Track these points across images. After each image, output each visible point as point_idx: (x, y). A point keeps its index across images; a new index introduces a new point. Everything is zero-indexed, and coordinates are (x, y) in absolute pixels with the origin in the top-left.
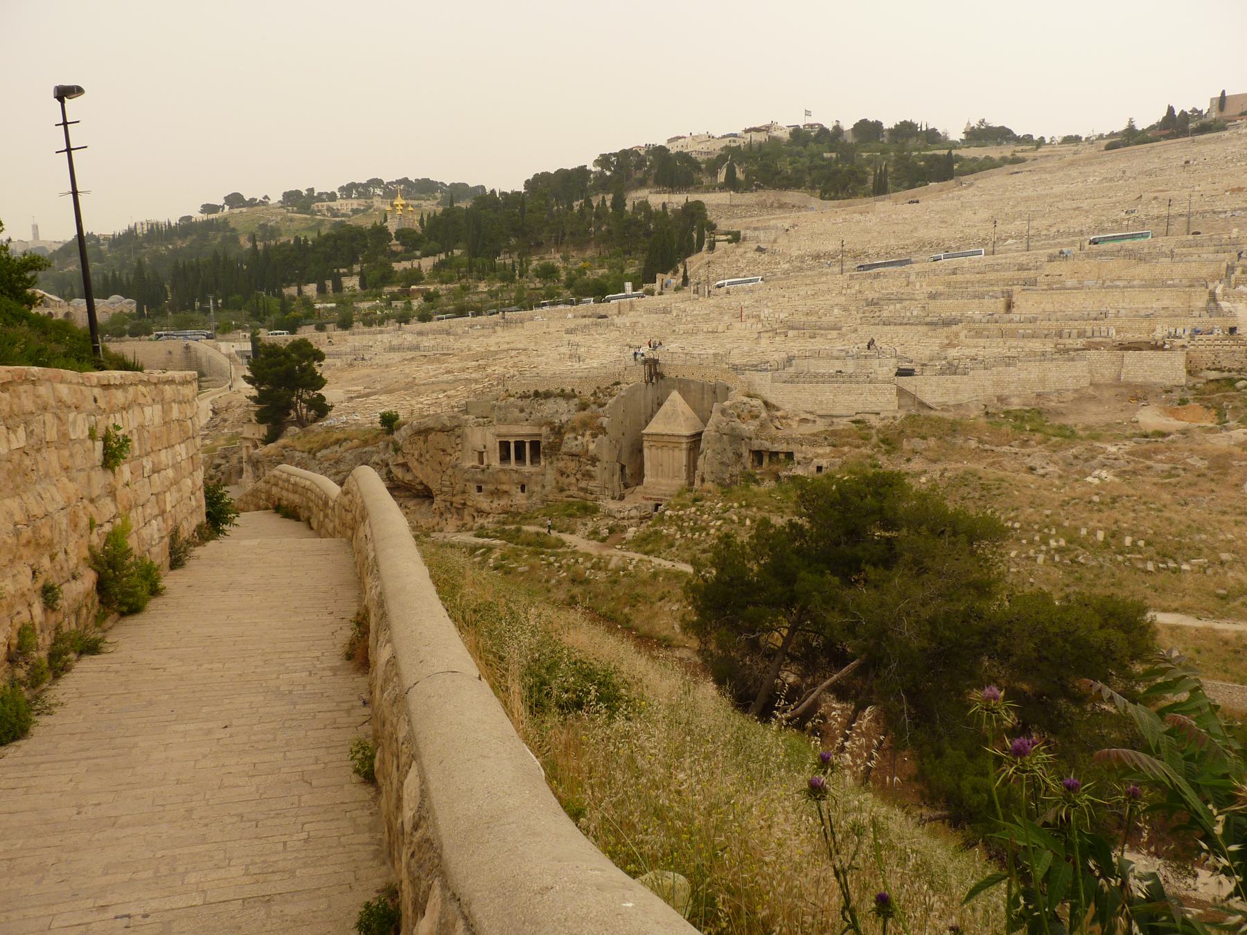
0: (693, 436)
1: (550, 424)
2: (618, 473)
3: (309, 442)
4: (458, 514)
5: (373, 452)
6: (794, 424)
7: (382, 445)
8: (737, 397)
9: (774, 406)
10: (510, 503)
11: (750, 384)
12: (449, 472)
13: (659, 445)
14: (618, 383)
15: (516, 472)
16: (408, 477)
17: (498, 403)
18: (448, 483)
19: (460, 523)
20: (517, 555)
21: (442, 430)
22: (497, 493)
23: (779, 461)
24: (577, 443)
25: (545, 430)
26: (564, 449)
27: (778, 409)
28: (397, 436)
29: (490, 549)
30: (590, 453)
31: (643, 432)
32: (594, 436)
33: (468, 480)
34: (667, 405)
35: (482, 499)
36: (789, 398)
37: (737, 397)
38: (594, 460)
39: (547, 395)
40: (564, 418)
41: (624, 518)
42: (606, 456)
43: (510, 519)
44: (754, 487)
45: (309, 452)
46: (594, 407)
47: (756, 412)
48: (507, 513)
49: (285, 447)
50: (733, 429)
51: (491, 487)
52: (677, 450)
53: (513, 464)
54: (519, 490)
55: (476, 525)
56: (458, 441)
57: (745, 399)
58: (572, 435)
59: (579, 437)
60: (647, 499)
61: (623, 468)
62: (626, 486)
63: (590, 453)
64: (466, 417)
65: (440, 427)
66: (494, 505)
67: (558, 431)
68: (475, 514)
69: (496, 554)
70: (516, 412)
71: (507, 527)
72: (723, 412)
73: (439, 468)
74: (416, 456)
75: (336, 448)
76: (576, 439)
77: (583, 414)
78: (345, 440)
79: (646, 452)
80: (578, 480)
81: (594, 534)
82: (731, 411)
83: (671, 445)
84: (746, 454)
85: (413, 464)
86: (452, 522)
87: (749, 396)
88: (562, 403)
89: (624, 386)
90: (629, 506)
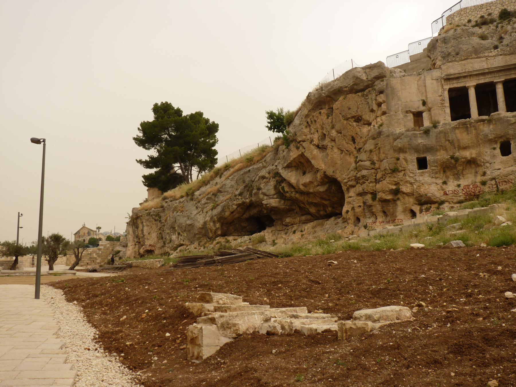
10: (479, 179)
18: (368, 163)
33: (401, 150)
51: (443, 156)
54: (498, 151)
56: (381, 98)
66: (451, 186)
70: (476, 40)
73: (351, 147)
75: (217, 180)
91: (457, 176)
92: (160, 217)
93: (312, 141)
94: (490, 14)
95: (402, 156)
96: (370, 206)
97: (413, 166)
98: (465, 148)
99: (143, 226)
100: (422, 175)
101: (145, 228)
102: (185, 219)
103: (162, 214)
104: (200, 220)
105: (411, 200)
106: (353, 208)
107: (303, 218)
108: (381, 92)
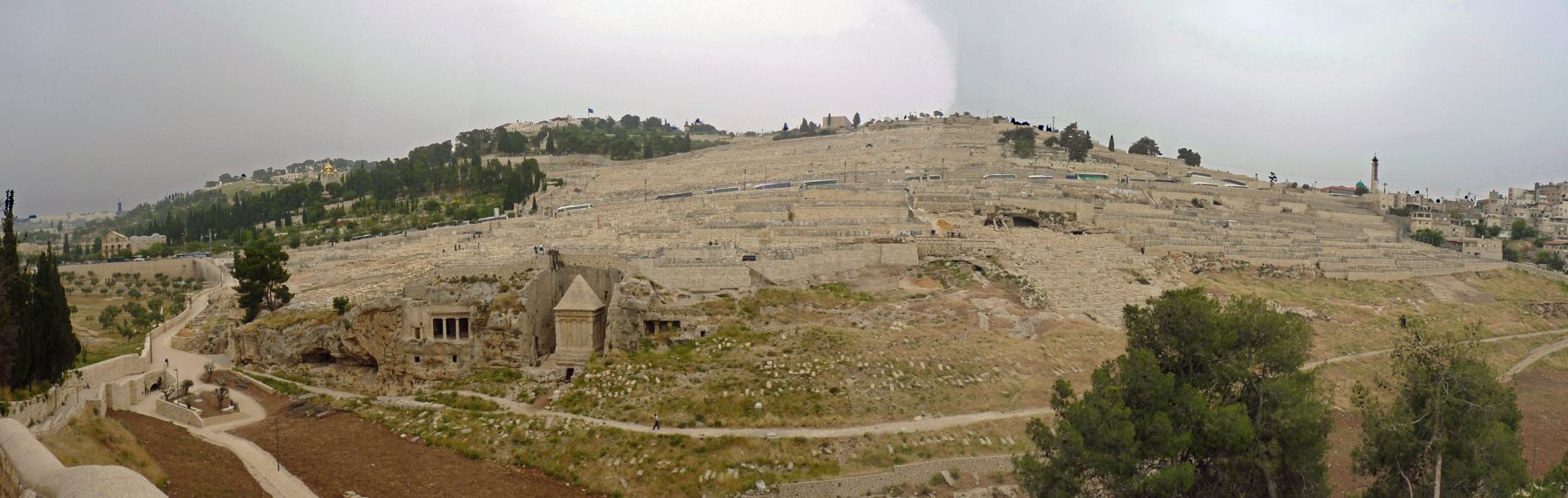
0: (597, 311)
1: (477, 304)
2: (533, 344)
3: (277, 322)
4: (399, 380)
5: (327, 329)
6: (675, 299)
7: (334, 323)
8: (629, 279)
9: (658, 286)
10: (443, 371)
11: (637, 269)
12: (392, 345)
13: (569, 319)
14: (531, 270)
15: (449, 345)
16: (357, 349)
17: (432, 287)
18: (391, 355)
19: (400, 388)
20: (457, 417)
22: (432, 363)
23: (668, 329)
24: (501, 319)
25: (473, 309)
26: (490, 324)
27: (661, 288)
28: (346, 316)
29: (432, 412)
30: (513, 327)
31: (555, 308)
32: (516, 313)
33: (407, 352)
34: (573, 287)
35: (419, 368)
36: (668, 279)
37: (629, 279)
38: (517, 333)
39: (473, 280)
40: (489, 299)
41: (544, 382)
42: (525, 330)
43: (445, 385)
44: (651, 350)
45: (277, 329)
46: (513, 289)
47: (646, 291)
48: (441, 380)
49: (259, 325)
50: (631, 304)
51: (427, 358)
52: (584, 323)
53: (445, 338)
55: (414, 391)
56: (399, 319)
57: (636, 280)
58: (497, 313)
59: (503, 314)
60: (560, 365)
61: (537, 338)
62: (539, 355)
63: (513, 327)
64: (406, 299)
66: (430, 373)
67: (484, 310)
68: (414, 381)
69: (438, 417)
70: (448, 294)
71: (443, 392)
72: (622, 290)
73: (382, 341)
75: (298, 326)
76: (500, 316)
77: (504, 295)
78: (305, 319)
79: (557, 325)
80: (502, 351)
81: (522, 397)
82: (627, 290)
83: (578, 319)
84: (641, 324)
85: (361, 338)
86: (394, 387)
87: (638, 278)
88: (486, 287)
89: (536, 272)
90: (548, 371)
91: (434, 367)
93: (361, 331)
95: (407, 355)
98: (438, 355)
104: (289, 352)
108: (399, 315)
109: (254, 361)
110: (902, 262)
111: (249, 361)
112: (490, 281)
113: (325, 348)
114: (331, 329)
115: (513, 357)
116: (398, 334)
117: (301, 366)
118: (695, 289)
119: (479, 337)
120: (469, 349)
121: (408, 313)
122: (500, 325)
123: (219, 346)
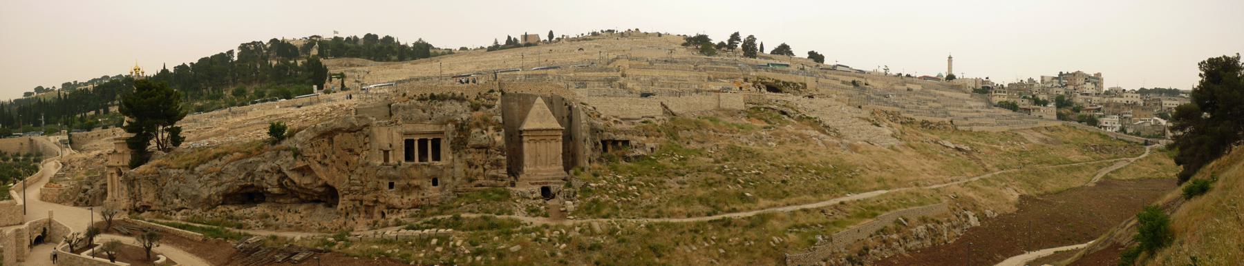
1: (454, 122)
5: (259, 162)
10: (420, 197)
12: (360, 170)
13: (538, 138)
16: (307, 180)
18: (358, 182)
21: (349, 131)
22: (407, 189)
26: (472, 142)
33: (381, 177)
35: (393, 195)
39: (443, 98)
40: (465, 117)
45: (187, 168)
48: (416, 207)
51: (403, 183)
54: (431, 183)
55: (391, 221)
56: (367, 140)
58: (478, 130)
60: (533, 184)
65: (348, 126)
66: (405, 200)
73: (345, 168)
74: (319, 159)
75: (217, 161)
78: (225, 154)
79: (526, 146)
80: (485, 170)
83: (548, 138)
85: (316, 166)
88: (458, 106)
91: (408, 194)
92: (157, 181)
93: (315, 158)
94: (425, 94)
95: (381, 181)
96: (357, 208)
97: (386, 187)
98: (414, 179)
99: (140, 187)
100: (391, 192)
101: (142, 189)
102: (190, 190)
103: (158, 179)
104: (205, 193)
105: (384, 206)
106: (346, 208)
107: (293, 200)
108: (367, 136)
109: (153, 208)
110: (733, 107)
111: (146, 208)
112: (461, 99)
113: (255, 184)
114: (264, 162)
115: (499, 175)
116: (366, 158)
117: (220, 208)
118: (624, 117)
119: (460, 156)
120: (451, 170)
121: (377, 133)
122: (485, 142)
123: (95, 198)
